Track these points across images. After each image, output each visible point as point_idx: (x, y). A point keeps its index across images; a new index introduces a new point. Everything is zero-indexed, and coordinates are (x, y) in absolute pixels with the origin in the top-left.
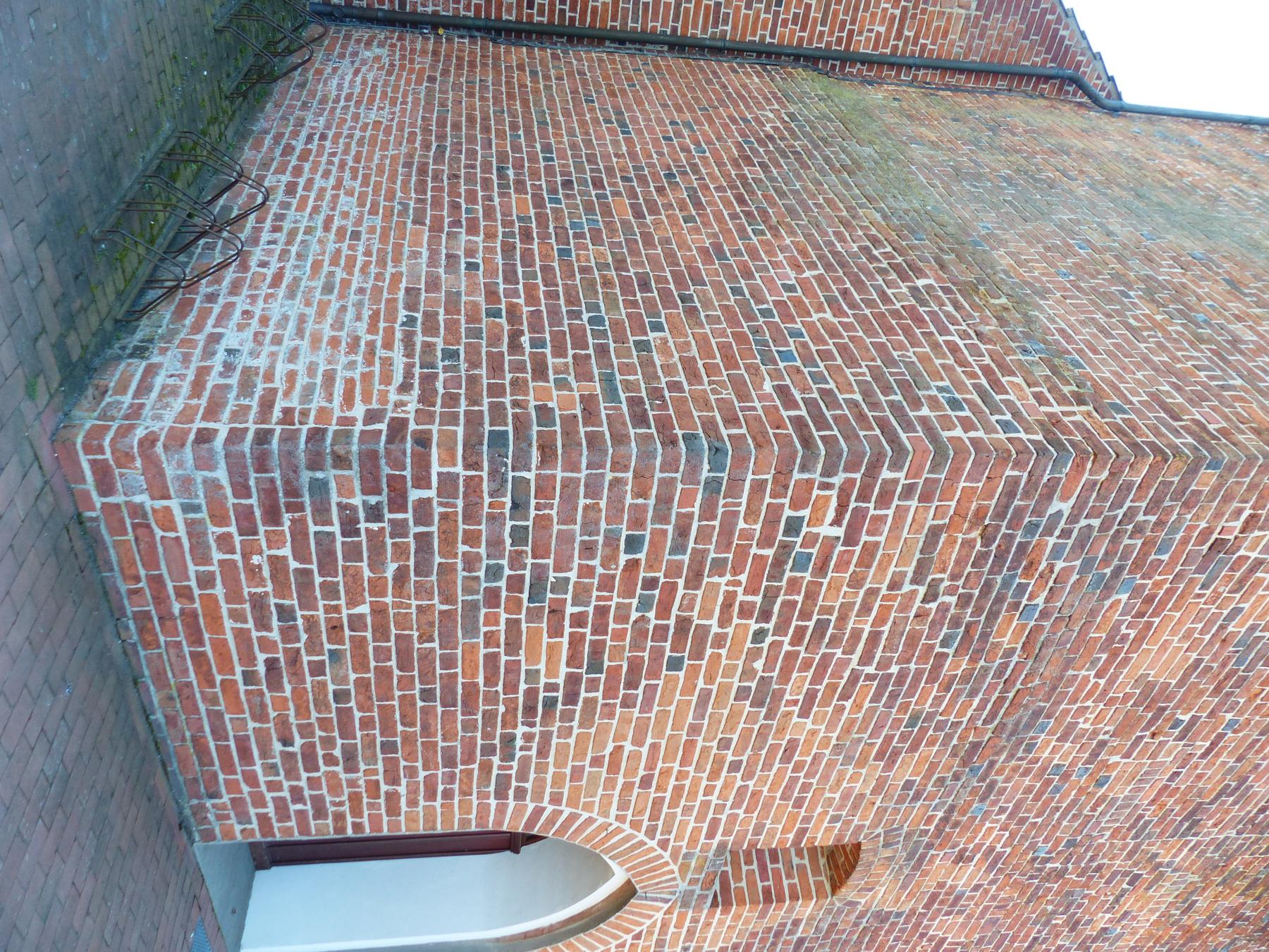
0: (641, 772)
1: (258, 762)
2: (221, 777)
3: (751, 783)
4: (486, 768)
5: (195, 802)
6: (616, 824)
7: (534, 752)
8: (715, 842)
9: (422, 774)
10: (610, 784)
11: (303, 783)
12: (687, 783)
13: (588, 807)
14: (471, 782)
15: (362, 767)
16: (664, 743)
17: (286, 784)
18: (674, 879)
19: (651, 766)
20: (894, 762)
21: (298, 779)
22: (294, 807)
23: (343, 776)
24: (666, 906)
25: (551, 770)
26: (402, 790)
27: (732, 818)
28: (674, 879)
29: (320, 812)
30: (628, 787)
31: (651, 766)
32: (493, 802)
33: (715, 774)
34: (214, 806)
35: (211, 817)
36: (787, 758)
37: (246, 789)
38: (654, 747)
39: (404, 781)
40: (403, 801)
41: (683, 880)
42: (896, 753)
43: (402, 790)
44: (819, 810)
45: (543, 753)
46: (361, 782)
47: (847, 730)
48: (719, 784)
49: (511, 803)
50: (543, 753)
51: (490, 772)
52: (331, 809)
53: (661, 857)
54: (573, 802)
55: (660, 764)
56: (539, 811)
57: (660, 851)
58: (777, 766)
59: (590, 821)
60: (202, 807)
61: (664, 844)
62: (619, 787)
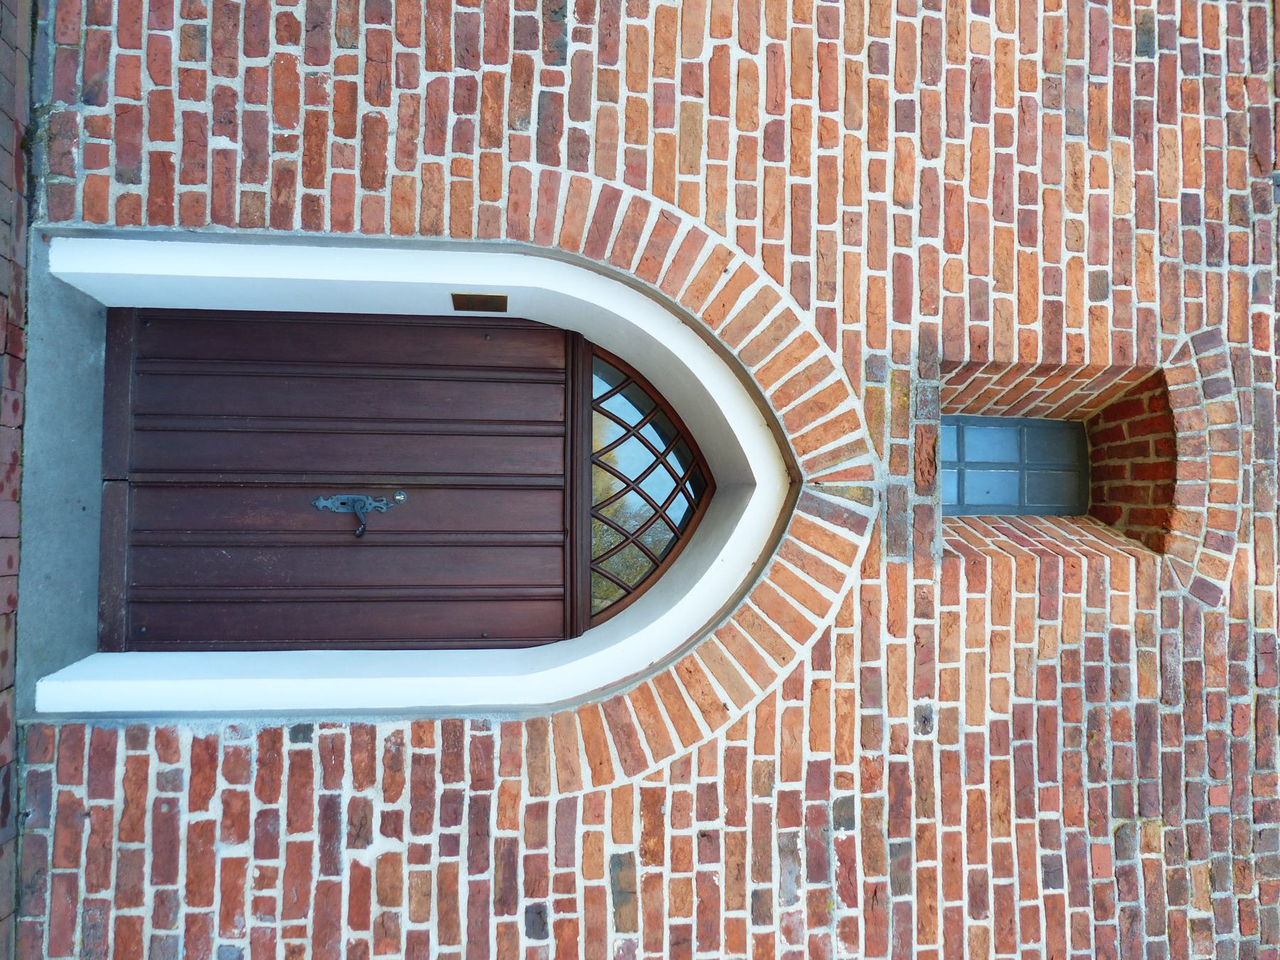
0: (764, 118)
1: (178, 22)
2: (115, 50)
3: (938, 164)
4: (523, 71)
5: (61, 106)
6: (740, 257)
7: (593, 47)
8: (913, 328)
9: (426, 77)
10: (719, 149)
11: (237, 84)
12: (838, 152)
13: (688, 204)
14: (500, 107)
15: (336, 52)
16: (786, 45)
17: (212, 82)
18: (859, 446)
19: (776, 105)
20: (1148, 138)
21: (232, 72)
22: (218, 142)
23: (302, 69)
24: (863, 542)
25: (624, 92)
26: (391, 114)
27: (927, 251)
28: (859, 446)
29: (254, 168)
30: (746, 146)
31: (776, 105)
32: (534, 167)
33: (876, 141)
34: (89, 122)
35: (77, 154)
36: (981, 113)
37: (147, 85)
38: (773, 52)
39: (395, 93)
40: (391, 142)
41: (878, 449)
42: (1144, 118)
43: (391, 114)
44: (1066, 256)
45: (609, 51)
46: (329, 87)
47: (1053, 44)
48: (888, 156)
49: (565, 174)
50: (609, 51)
51: (528, 84)
52: (275, 157)
53: (825, 366)
54: (664, 192)
55: (789, 102)
56: (610, 198)
57: (823, 349)
58: (969, 126)
59: (696, 238)
60: (69, 119)
61: (826, 321)
62: (733, 150)
